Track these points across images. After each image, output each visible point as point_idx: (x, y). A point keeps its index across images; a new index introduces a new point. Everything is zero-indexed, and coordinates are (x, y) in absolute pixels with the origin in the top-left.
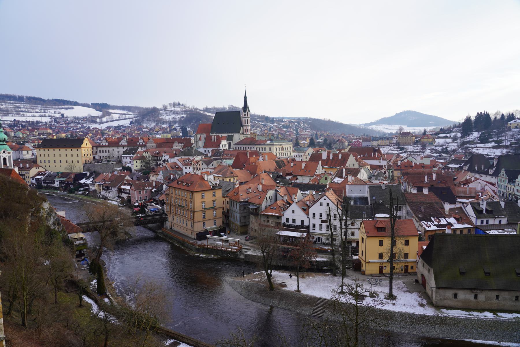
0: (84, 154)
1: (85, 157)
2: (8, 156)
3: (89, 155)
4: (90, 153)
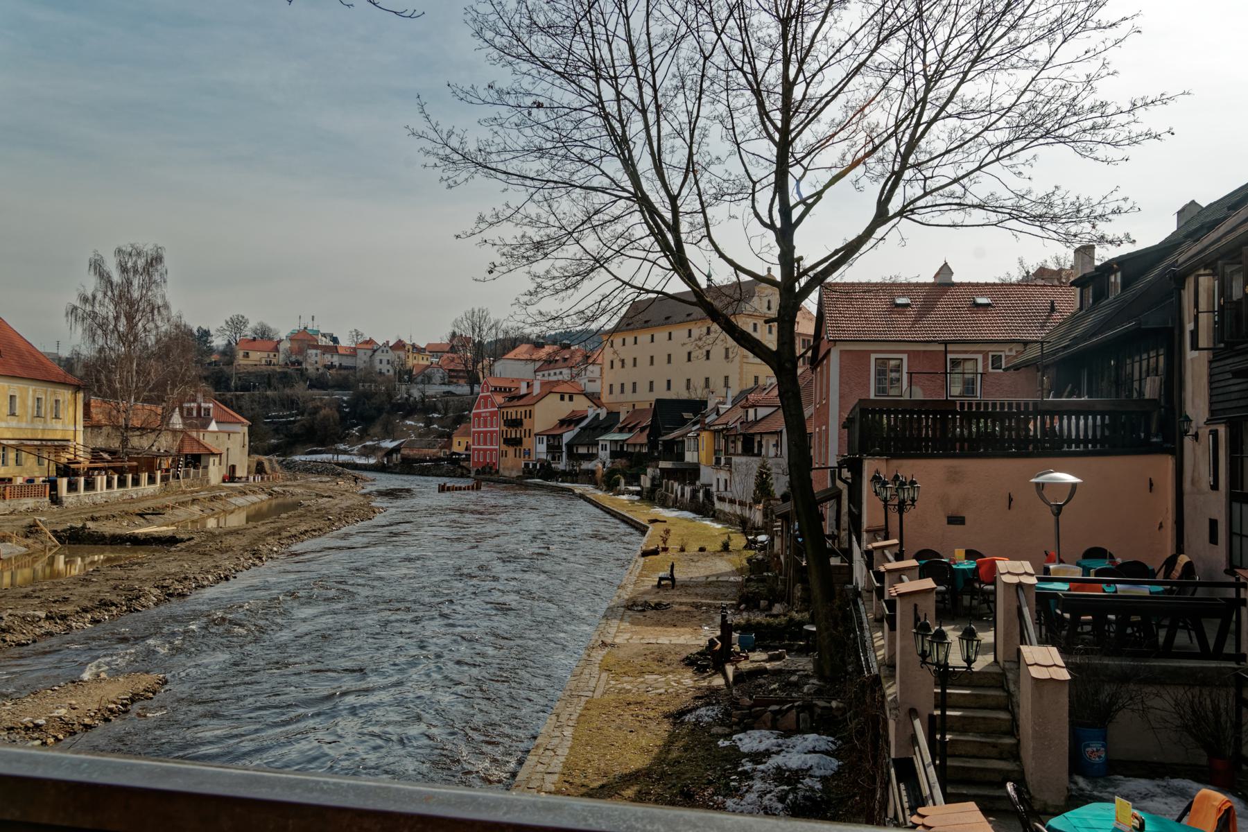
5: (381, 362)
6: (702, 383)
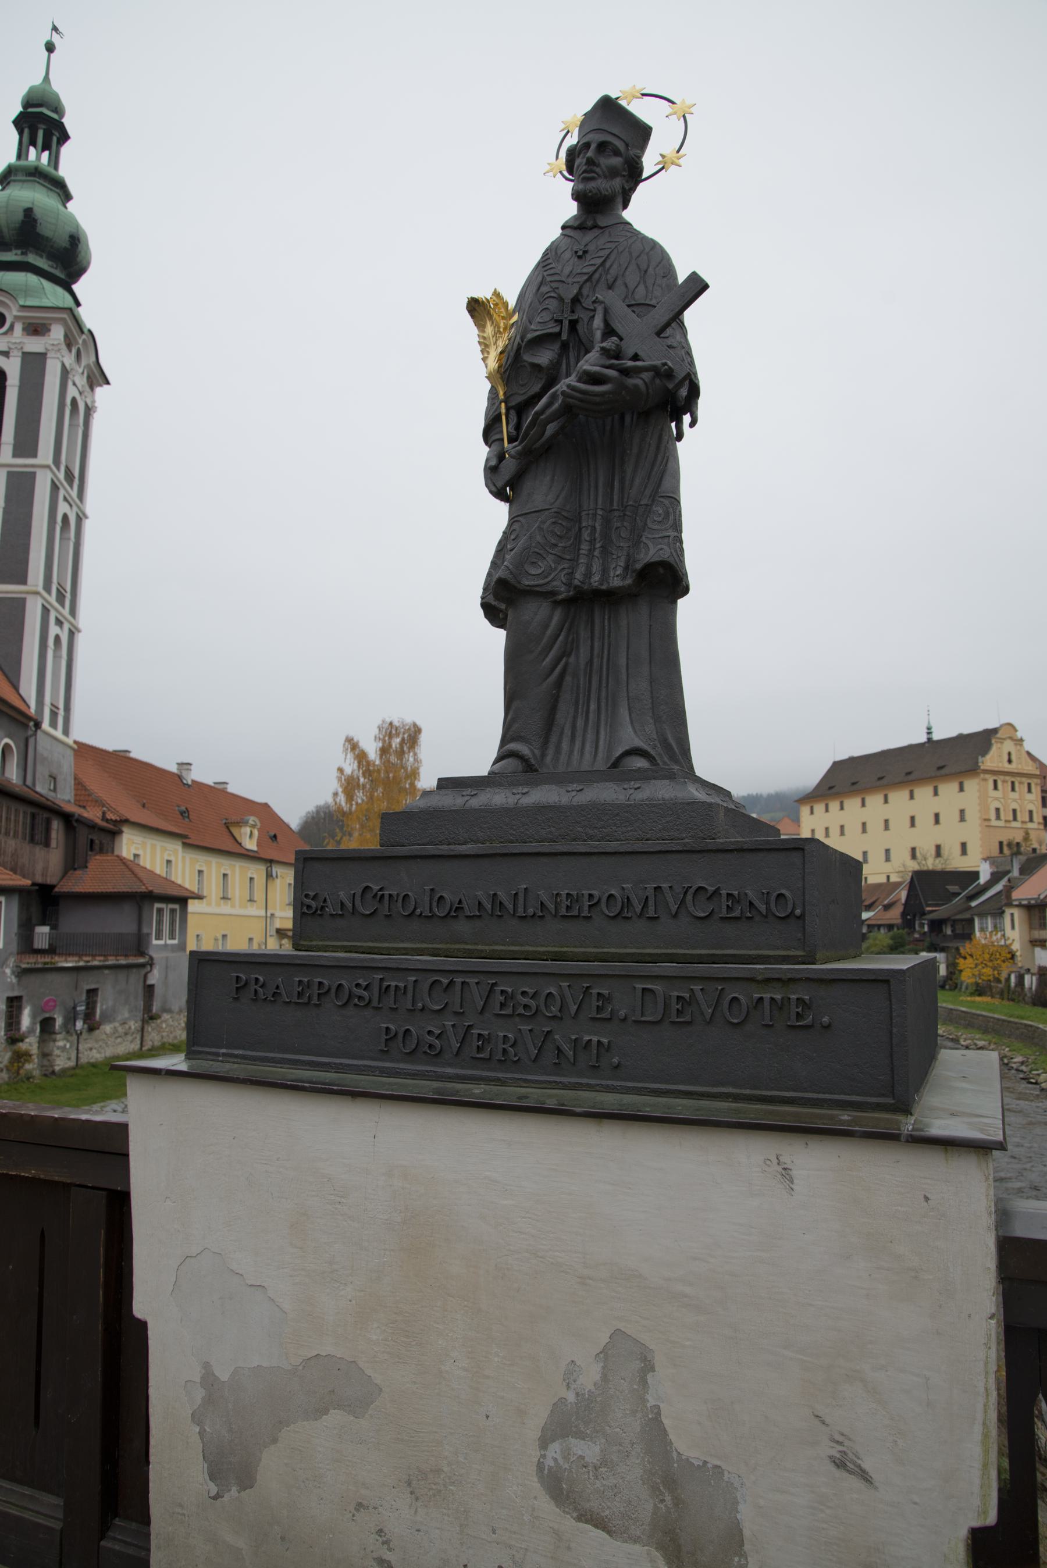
0: (997, 804)
1: (1001, 823)
2: (26, 356)
3: (1023, 816)
4: (1031, 807)
6: (933, 851)
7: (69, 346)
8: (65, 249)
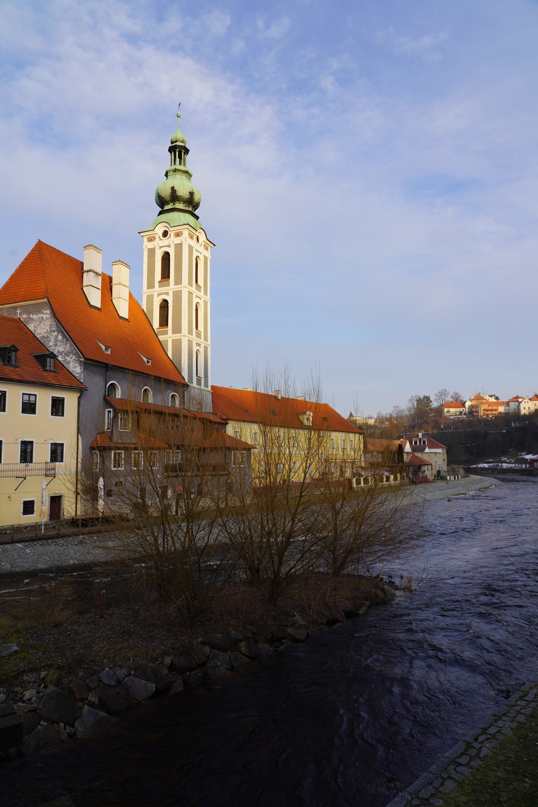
5: (524, 409)
7: (191, 237)
8: (189, 198)
